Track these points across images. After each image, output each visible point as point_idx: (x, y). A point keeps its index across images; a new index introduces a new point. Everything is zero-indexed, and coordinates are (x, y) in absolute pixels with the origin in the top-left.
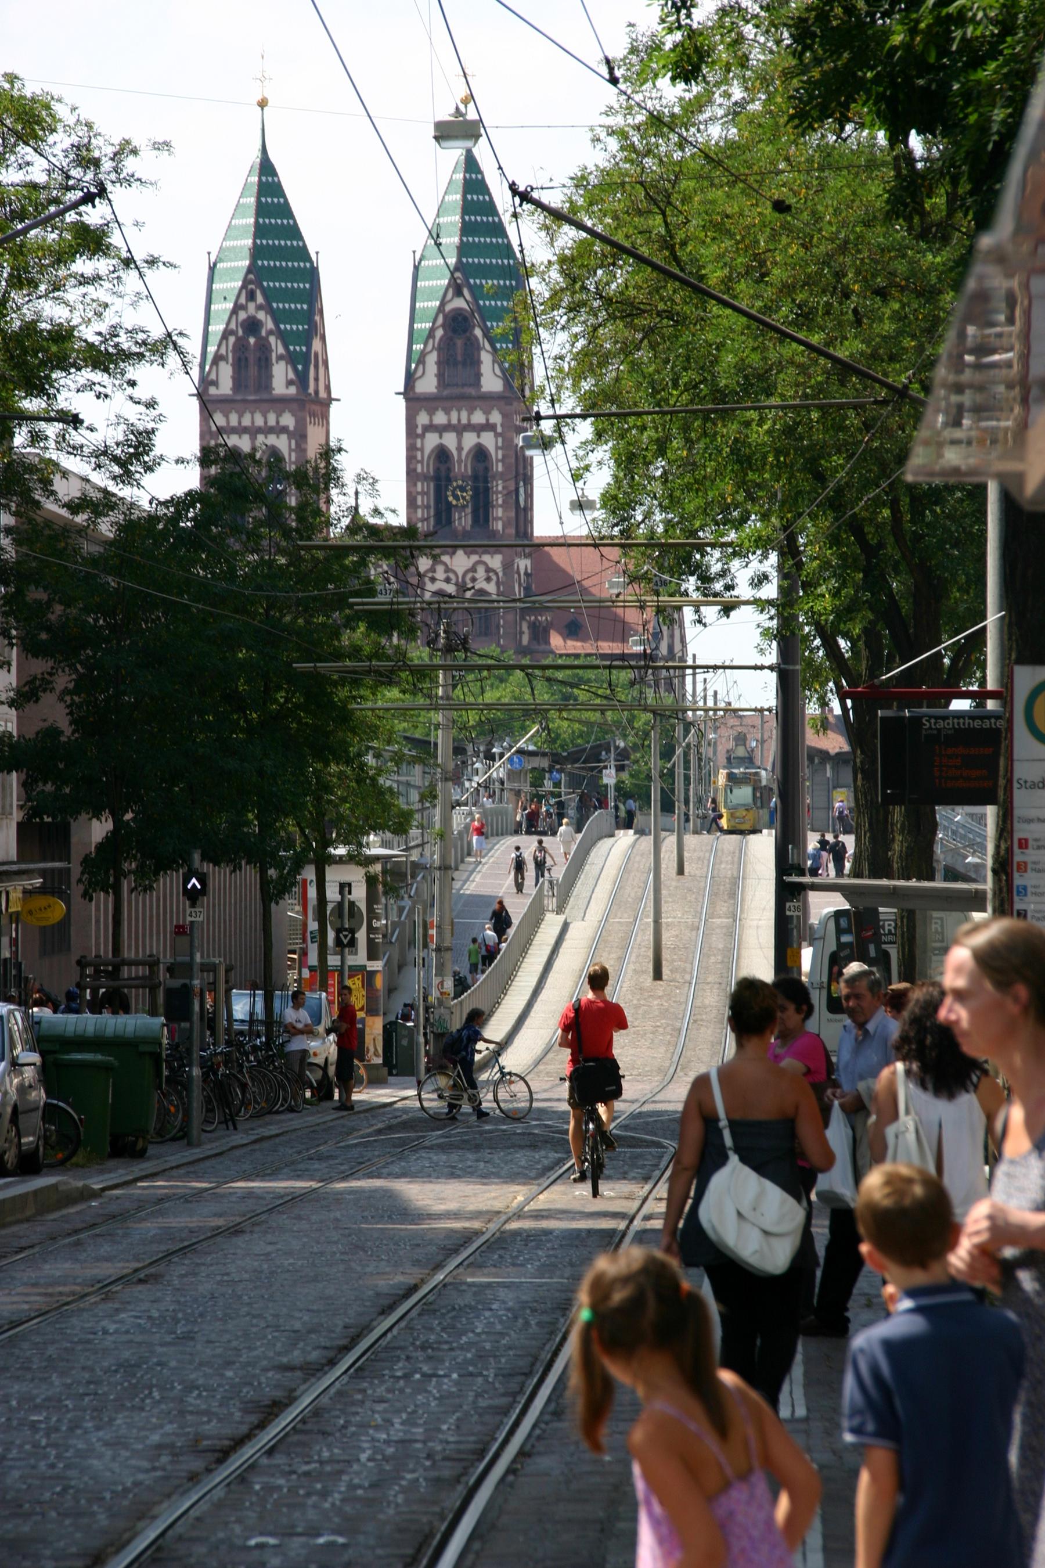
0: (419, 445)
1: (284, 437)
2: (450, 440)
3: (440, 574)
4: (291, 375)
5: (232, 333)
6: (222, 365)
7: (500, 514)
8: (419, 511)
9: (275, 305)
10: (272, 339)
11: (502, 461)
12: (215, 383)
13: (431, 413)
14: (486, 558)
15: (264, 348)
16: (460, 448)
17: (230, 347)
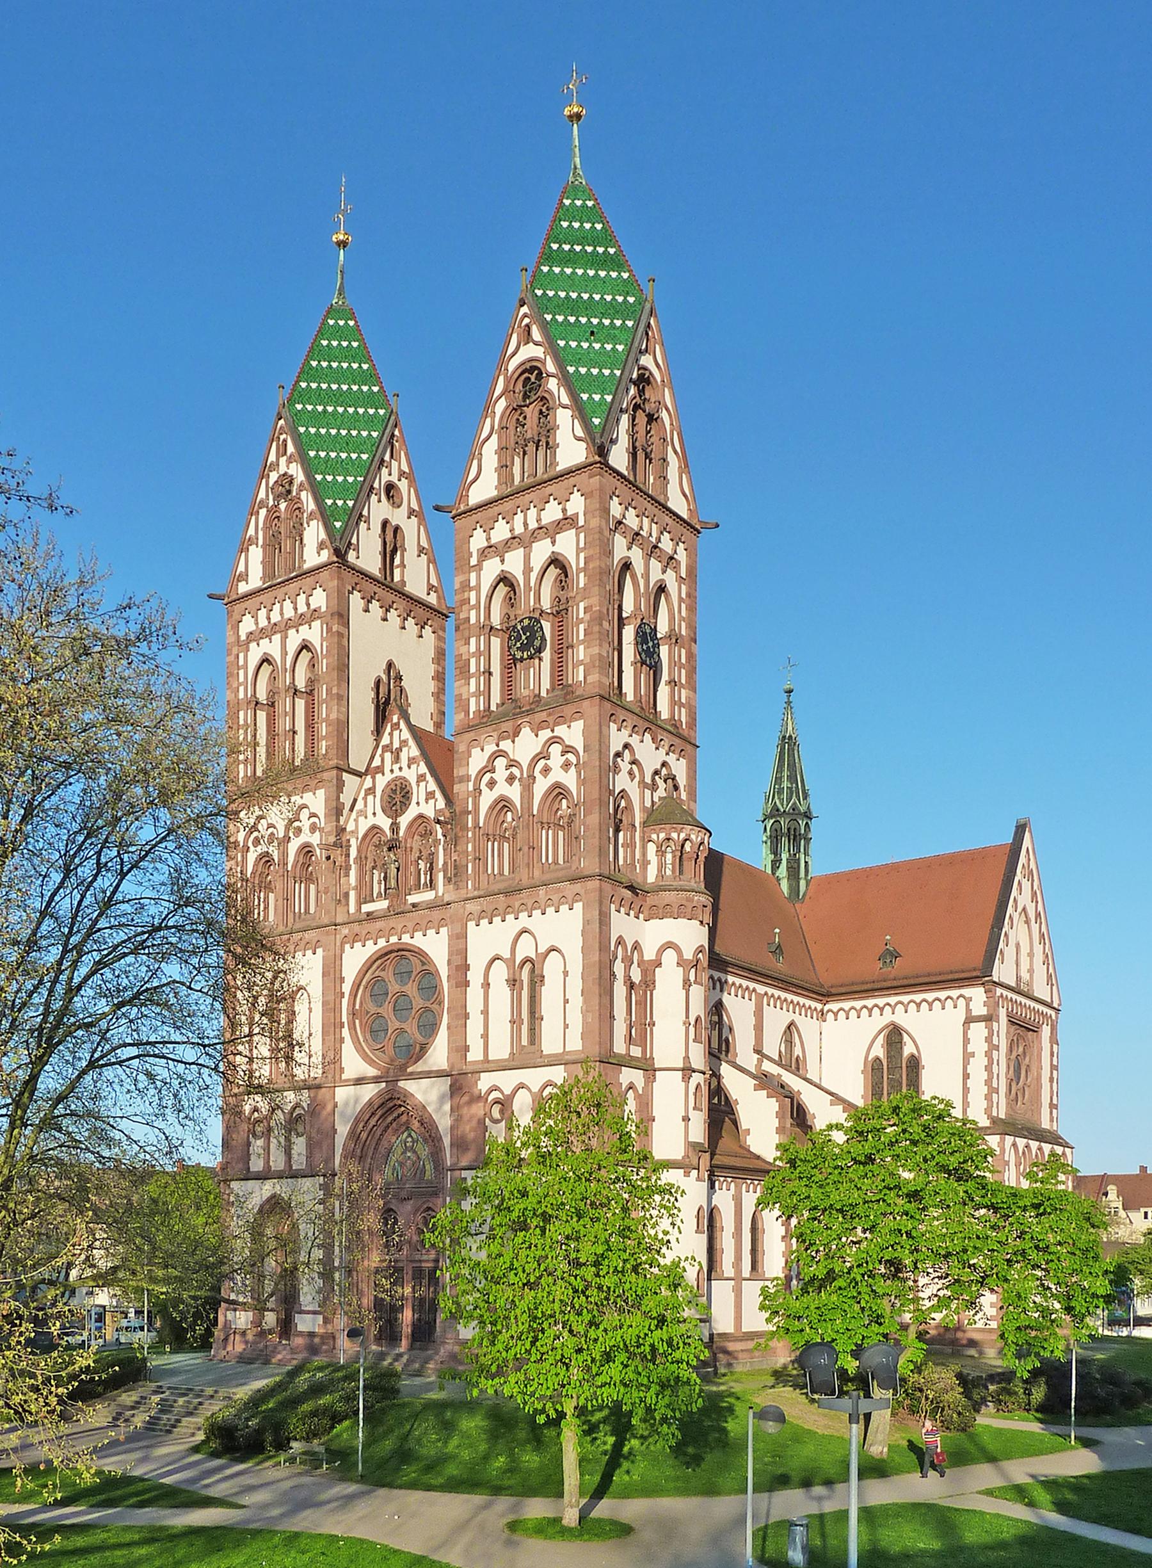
0: (473, 583)
1: (316, 624)
2: (514, 564)
3: (501, 774)
4: (323, 535)
5: (262, 504)
6: (252, 548)
7: (581, 657)
8: (473, 681)
9: (312, 454)
10: (303, 494)
11: (585, 569)
12: (244, 577)
13: (488, 530)
14: (561, 731)
15: (297, 508)
16: (528, 570)
17: (261, 525)
